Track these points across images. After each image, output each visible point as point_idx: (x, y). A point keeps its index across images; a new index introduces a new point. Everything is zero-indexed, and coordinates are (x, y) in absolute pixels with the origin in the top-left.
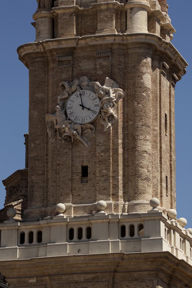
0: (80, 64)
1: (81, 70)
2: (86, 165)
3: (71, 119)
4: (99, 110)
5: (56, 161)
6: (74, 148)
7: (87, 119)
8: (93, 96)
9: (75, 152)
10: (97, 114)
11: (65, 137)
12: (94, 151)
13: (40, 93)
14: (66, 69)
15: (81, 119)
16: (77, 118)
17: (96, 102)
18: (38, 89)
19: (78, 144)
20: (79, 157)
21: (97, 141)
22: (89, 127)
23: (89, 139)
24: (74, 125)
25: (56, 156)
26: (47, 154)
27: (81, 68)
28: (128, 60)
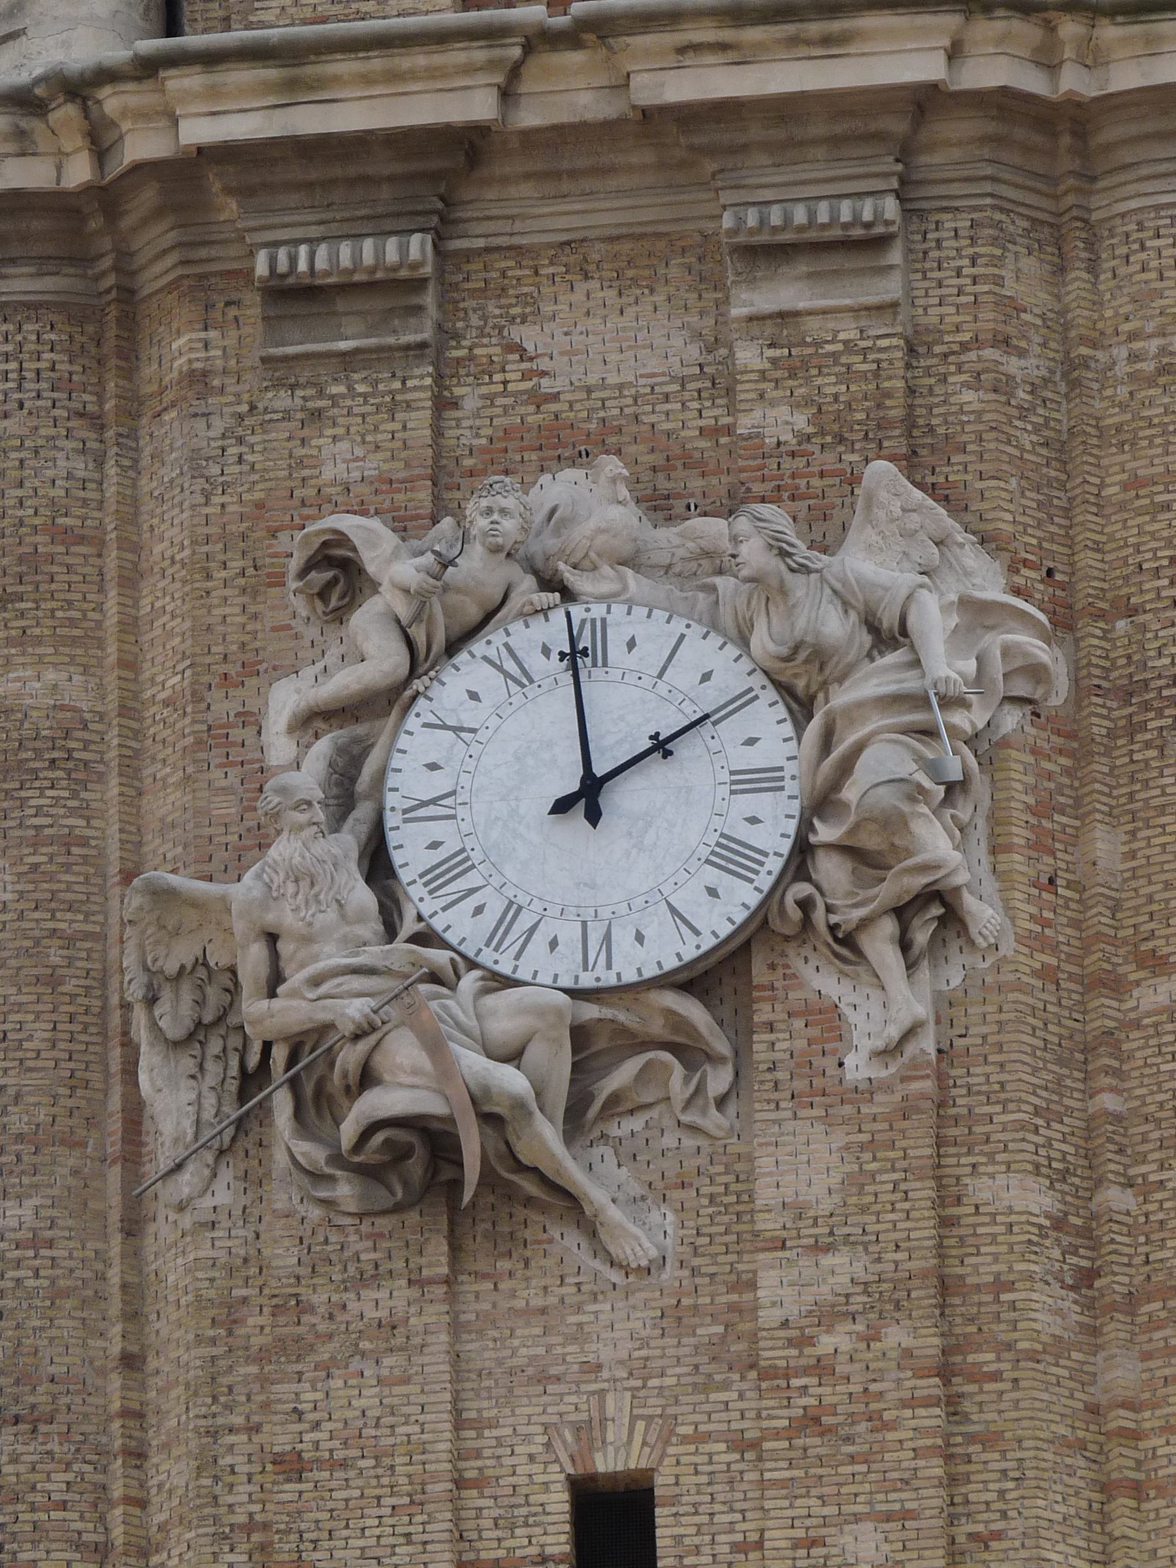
0: (528, 336)
1: (539, 400)
2: (628, 1473)
3: (452, 938)
4: (791, 827)
5: (257, 1429)
6: (479, 1276)
7: (640, 938)
8: (706, 677)
9: (494, 1324)
10: (766, 882)
11: (379, 1138)
12: (732, 1308)
13: (40, 660)
14: (361, 388)
15: (569, 933)
16: (525, 921)
17: (751, 742)
18: (22, 615)
19: (528, 1234)
20: (544, 1379)
21: (765, 1194)
22: (657, 1028)
23: (655, 1177)
24: (490, 1000)
25: (253, 1369)
26: (134, 1349)
27: (544, 374)
28: (1098, 305)
